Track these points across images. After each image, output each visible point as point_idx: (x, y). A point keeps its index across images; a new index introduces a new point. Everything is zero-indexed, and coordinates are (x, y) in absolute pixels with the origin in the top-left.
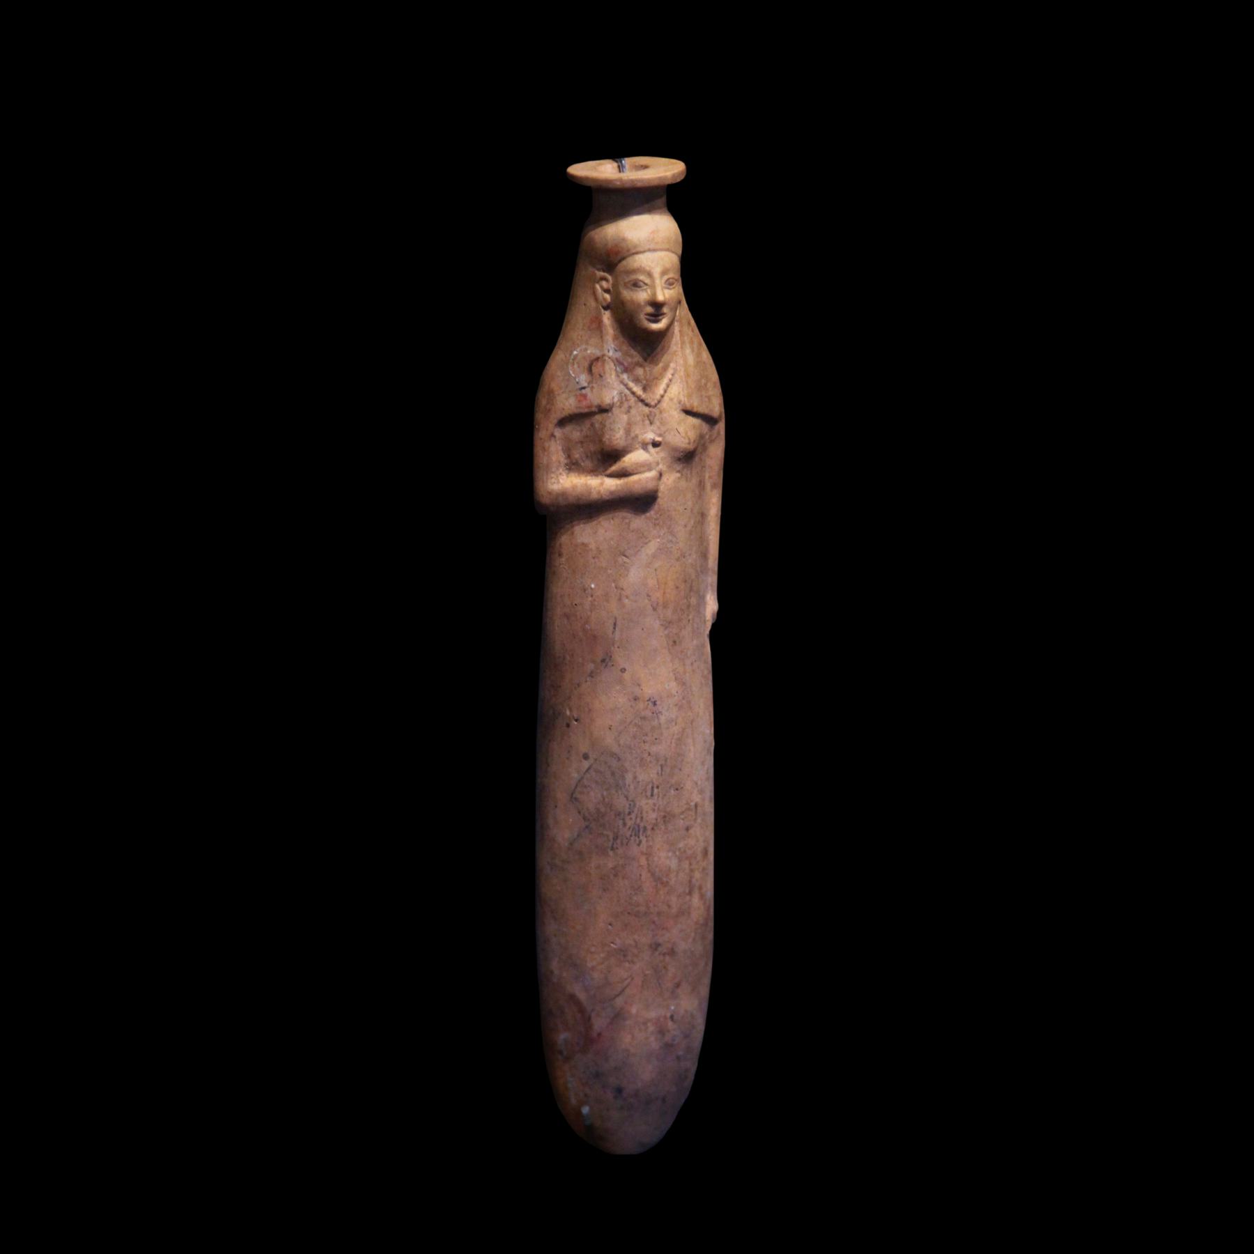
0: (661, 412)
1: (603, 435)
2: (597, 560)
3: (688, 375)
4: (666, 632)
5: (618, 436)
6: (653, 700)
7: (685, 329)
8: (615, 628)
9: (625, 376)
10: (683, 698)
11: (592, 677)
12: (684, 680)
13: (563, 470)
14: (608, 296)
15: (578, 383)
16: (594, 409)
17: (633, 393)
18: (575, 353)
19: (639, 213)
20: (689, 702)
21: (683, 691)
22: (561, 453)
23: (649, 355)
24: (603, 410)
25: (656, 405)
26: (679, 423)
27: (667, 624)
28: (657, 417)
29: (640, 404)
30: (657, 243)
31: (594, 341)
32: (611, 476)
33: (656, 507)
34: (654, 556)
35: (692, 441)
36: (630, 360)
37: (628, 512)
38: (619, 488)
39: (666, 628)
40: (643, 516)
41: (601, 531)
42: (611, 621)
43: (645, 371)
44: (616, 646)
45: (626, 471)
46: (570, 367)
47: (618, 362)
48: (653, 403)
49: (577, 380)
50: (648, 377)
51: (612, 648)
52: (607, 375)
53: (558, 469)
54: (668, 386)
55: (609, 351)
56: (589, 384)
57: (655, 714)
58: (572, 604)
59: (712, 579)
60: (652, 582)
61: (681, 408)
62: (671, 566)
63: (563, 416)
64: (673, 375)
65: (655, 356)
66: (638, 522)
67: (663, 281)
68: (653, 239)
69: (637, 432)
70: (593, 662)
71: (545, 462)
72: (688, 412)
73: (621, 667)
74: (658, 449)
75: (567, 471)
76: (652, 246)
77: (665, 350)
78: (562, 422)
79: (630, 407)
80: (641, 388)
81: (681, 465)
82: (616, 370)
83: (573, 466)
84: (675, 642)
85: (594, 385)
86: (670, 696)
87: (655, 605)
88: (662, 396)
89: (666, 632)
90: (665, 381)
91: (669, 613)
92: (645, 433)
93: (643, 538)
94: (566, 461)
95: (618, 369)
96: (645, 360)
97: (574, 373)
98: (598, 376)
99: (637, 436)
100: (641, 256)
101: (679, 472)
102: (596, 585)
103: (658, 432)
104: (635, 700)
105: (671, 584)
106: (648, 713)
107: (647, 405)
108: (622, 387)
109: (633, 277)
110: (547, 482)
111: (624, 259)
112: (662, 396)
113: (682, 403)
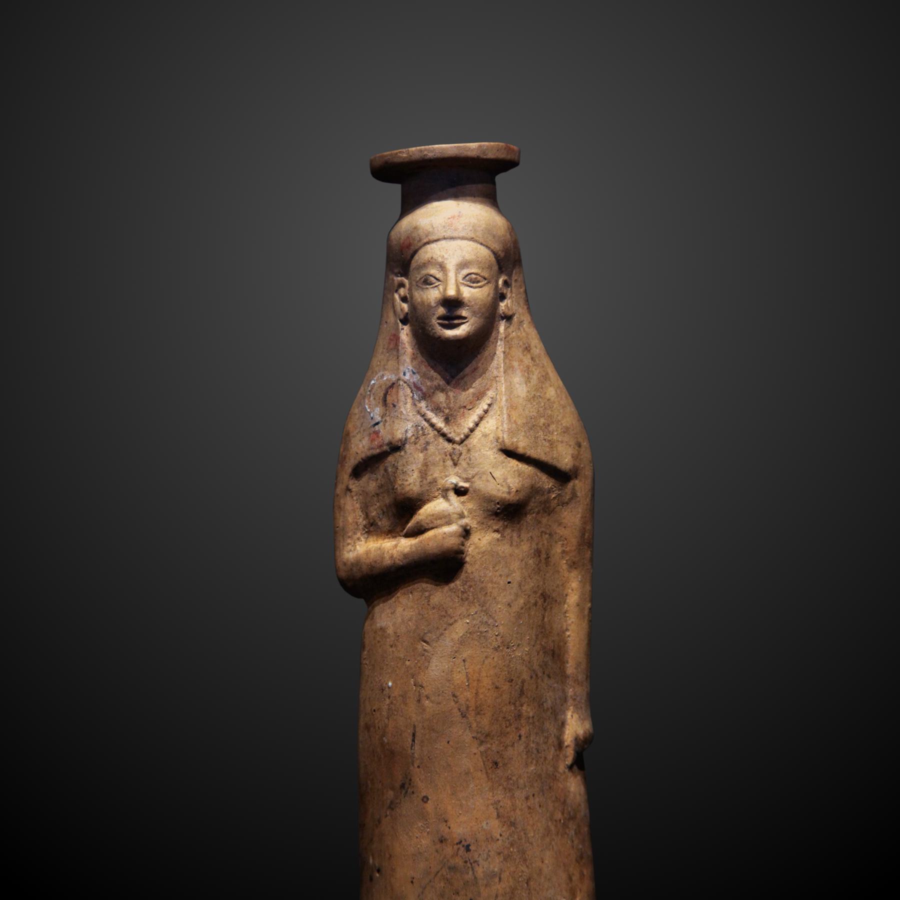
0: (469, 450)
1: (395, 481)
2: (394, 649)
3: (512, 407)
4: (482, 748)
5: (411, 480)
6: (466, 844)
7: (517, 353)
8: (413, 741)
9: (423, 404)
10: (512, 845)
11: (393, 809)
12: (512, 819)
13: (362, 534)
14: (405, 306)
15: (372, 418)
16: (385, 448)
17: (432, 425)
18: (373, 382)
19: (440, 199)
20: (523, 852)
21: (510, 835)
22: (359, 513)
23: (453, 377)
24: (396, 448)
25: (462, 441)
26: (495, 466)
27: (483, 738)
28: (462, 457)
29: (441, 440)
30: (456, 230)
31: (392, 363)
32: (407, 536)
33: (463, 575)
34: (462, 642)
35: (514, 490)
36: (429, 384)
37: (427, 583)
38: (414, 549)
39: (482, 743)
40: (446, 588)
41: (399, 610)
42: (410, 731)
43: (448, 397)
44: (416, 765)
45: (422, 526)
46: (367, 401)
47: (416, 387)
48: (457, 439)
49: (372, 415)
50: (452, 405)
51: (412, 768)
52: (401, 404)
53: (355, 533)
54: (481, 418)
55: (404, 374)
56: (382, 417)
57: (469, 865)
58: (371, 710)
59: (576, 691)
60: (459, 678)
61: (499, 447)
62: (486, 657)
63: (356, 462)
64: (490, 405)
65: (462, 378)
66: (440, 595)
67: (460, 277)
68: (451, 225)
69: (436, 475)
70: (393, 788)
71: (341, 524)
72: (509, 453)
73: (424, 794)
74: (463, 498)
75: (366, 536)
76: (449, 234)
77: (477, 373)
78: (358, 472)
79: (428, 443)
80: (442, 419)
81: (501, 523)
82: (413, 397)
83: (372, 529)
84: (496, 763)
85: (388, 418)
86: (490, 839)
87: (463, 708)
88: (472, 430)
89: (482, 748)
90: (479, 411)
91: (485, 721)
92: (446, 476)
93: (446, 618)
94: (364, 522)
95: (415, 396)
96: (448, 383)
97: (369, 408)
98: (392, 406)
99: (435, 481)
100: (433, 245)
101: (497, 531)
102: (393, 683)
103: (464, 476)
104: (441, 842)
105: (486, 682)
106: (459, 862)
107: (450, 440)
108: (419, 417)
109: (424, 272)
110: (343, 549)
111: (416, 252)
112: (472, 430)
113: (500, 441)
